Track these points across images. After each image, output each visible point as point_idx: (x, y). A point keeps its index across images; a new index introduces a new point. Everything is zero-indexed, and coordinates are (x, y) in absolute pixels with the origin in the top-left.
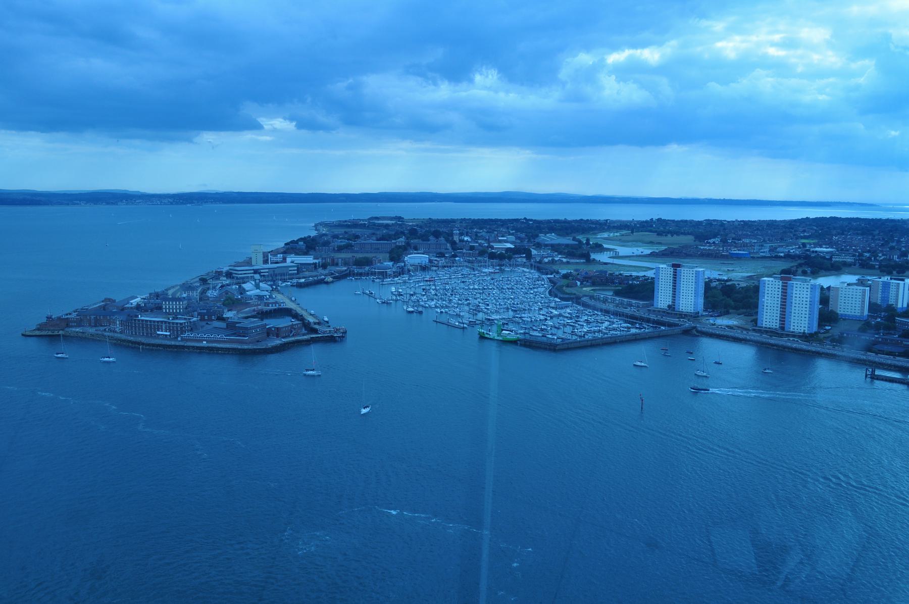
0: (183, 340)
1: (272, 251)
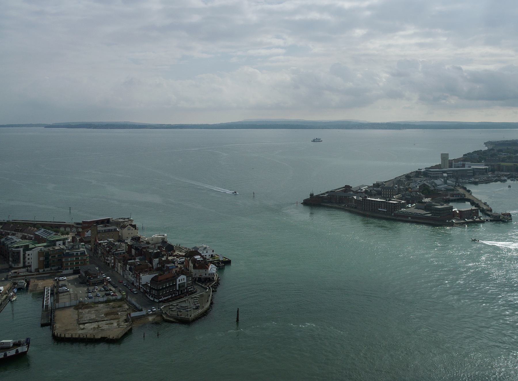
0: (395, 216)
1: (455, 159)
